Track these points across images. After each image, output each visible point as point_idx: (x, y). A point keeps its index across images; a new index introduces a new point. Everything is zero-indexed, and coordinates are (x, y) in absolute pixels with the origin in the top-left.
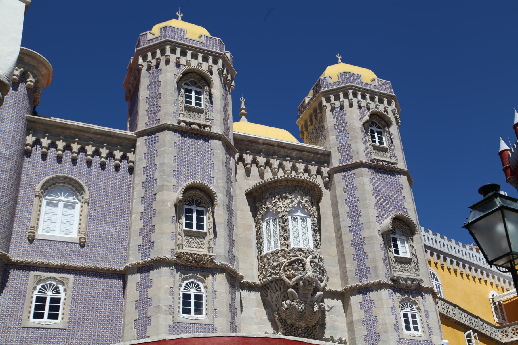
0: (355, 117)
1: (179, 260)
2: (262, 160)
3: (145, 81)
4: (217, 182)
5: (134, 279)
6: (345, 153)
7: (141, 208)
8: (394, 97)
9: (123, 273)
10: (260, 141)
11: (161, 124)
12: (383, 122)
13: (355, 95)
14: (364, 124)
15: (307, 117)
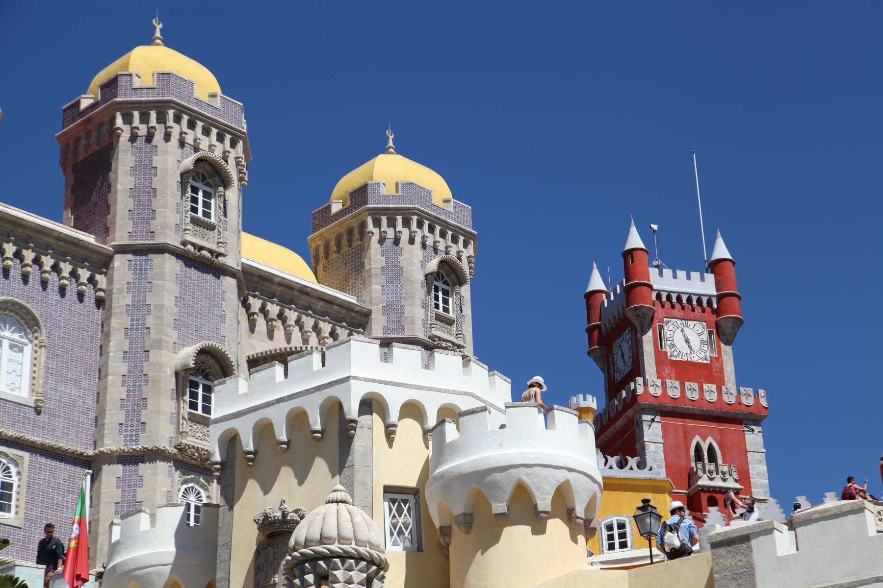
0: (417, 263)
1: (181, 454)
2: (273, 309)
3: (125, 159)
4: (229, 345)
5: (112, 473)
6: (393, 317)
7: (124, 368)
8: (474, 235)
9: (90, 459)
10: (276, 280)
11: (157, 241)
12: (453, 276)
13: (420, 225)
14: (426, 276)
15: (333, 237)
